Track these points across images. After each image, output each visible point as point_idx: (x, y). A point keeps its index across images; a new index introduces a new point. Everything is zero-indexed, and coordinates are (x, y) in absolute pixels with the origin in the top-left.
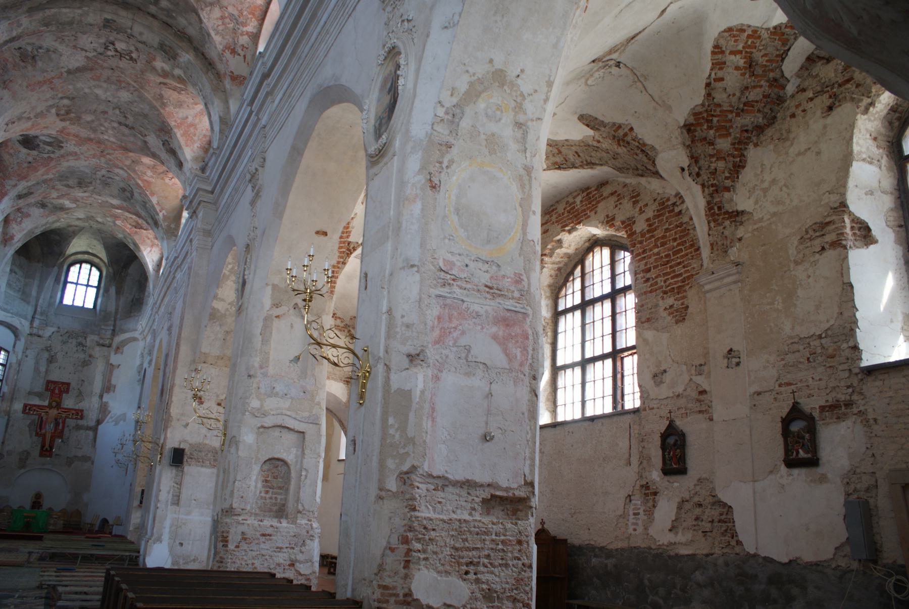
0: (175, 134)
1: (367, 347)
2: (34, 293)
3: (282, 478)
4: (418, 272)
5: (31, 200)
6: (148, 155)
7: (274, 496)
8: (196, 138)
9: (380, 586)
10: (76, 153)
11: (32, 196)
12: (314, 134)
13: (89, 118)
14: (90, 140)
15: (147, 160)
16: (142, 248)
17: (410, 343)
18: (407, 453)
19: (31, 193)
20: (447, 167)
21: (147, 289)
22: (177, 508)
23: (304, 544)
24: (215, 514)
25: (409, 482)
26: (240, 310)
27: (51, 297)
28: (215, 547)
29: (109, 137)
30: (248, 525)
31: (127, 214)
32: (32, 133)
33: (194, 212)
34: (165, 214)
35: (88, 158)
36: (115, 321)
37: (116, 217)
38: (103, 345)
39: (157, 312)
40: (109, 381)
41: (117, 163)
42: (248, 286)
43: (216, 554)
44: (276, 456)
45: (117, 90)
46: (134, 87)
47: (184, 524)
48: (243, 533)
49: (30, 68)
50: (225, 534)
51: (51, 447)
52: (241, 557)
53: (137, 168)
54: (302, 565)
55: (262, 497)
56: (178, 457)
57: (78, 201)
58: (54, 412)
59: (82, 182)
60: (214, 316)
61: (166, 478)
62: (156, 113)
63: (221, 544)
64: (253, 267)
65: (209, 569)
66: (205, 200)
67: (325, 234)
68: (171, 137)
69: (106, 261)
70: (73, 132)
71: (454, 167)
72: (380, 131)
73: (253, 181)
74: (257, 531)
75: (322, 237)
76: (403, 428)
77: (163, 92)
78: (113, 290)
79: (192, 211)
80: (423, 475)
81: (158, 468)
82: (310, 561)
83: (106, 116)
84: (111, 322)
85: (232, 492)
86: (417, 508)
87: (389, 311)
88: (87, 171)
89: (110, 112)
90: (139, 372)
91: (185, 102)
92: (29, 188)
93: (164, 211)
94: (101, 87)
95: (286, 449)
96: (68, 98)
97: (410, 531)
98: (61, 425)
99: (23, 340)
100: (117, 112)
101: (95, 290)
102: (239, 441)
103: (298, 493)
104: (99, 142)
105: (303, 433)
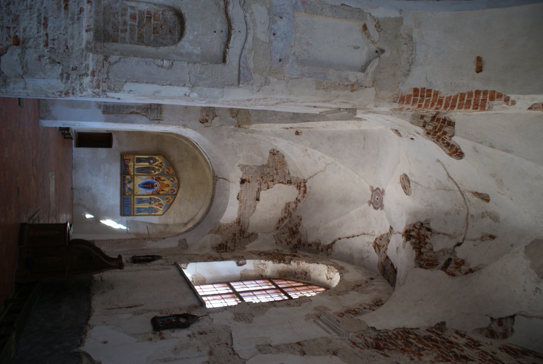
44: (187, 24)
55: (125, 9)
67: (479, 70)
105: (224, 61)
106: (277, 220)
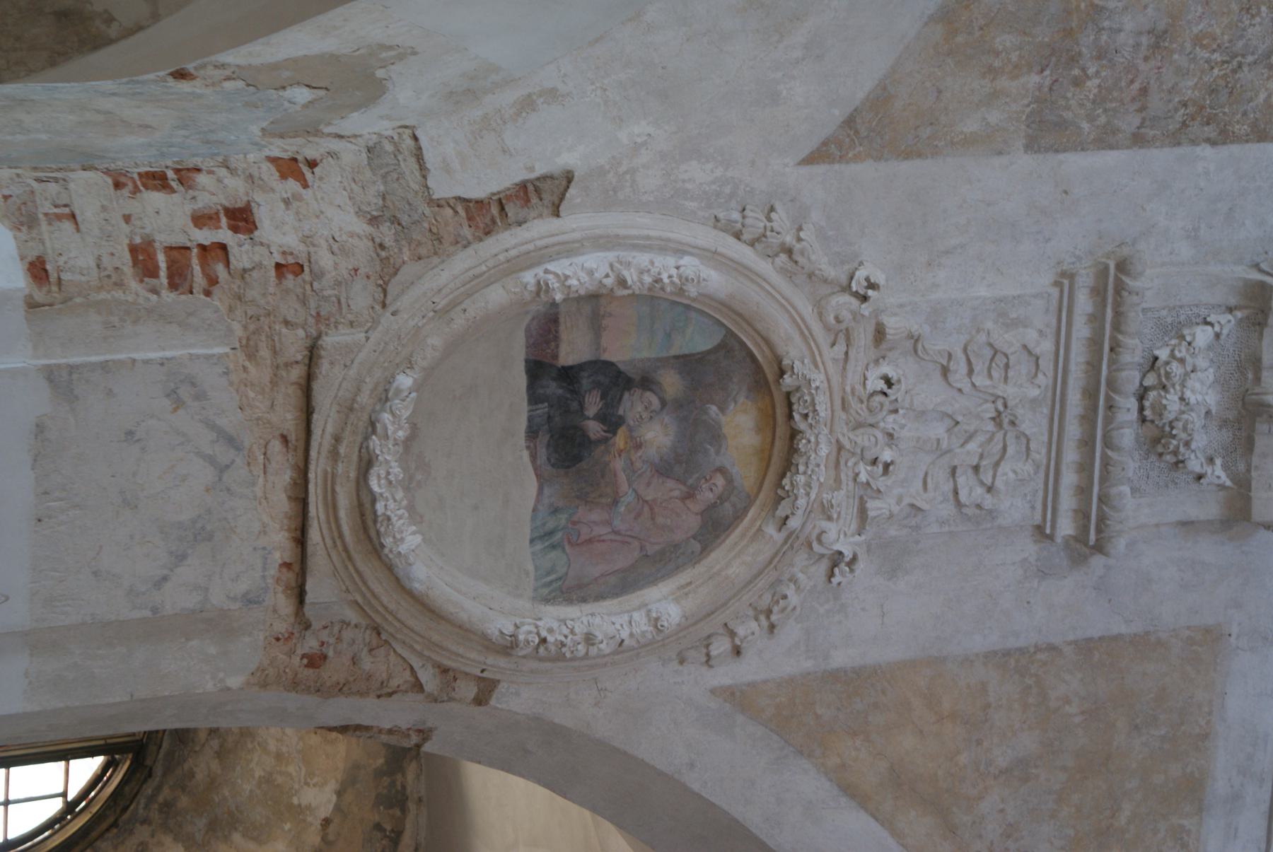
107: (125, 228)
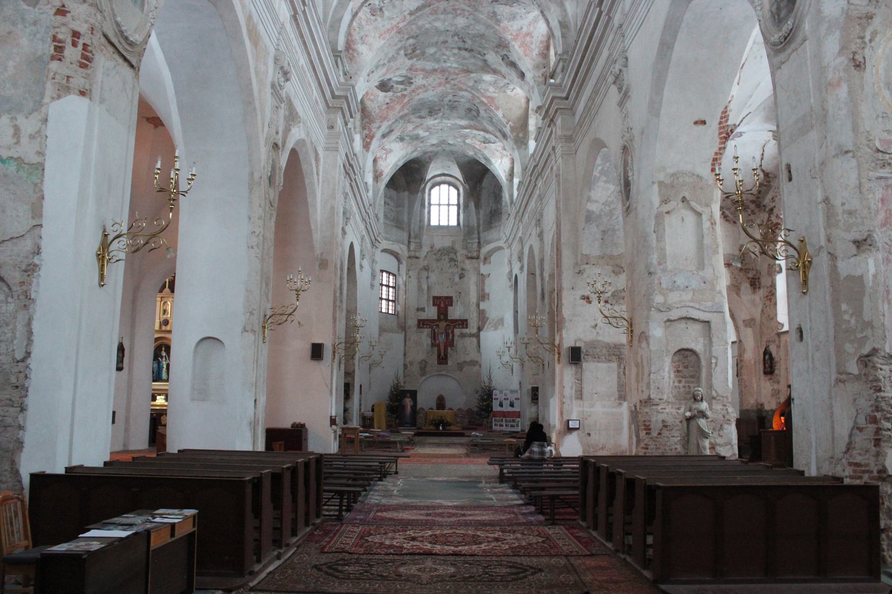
0: (513, 46)
1: (804, 237)
2: (406, 219)
3: (693, 367)
4: (853, 157)
5: (393, 136)
6: (488, 72)
7: (687, 385)
8: (533, 46)
9: (850, 464)
10: (424, 86)
11: (393, 133)
12: (683, 25)
13: (431, 50)
14: (435, 70)
15: (488, 78)
16: (493, 161)
17: (855, 229)
18: (865, 337)
19: (392, 131)
20: (871, 41)
21: (503, 199)
22: (581, 402)
23: (721, 428)
24: (632, 405)
25: (871, 364)
26: (628, 210)
27: (420, 221)
28: (638, 436)
29: (452, 64)
30: (667, 413)
31: (475, 132)
32: (387, 77)
33: (552, 120)
34: (512, 125)
35: (435, 87)
36: (479, 233)
37: (465, 137)
38: (472, 258)
39: (520, 220)
40: (483, 290)
41: (461, 86)
42: (634, 188)
43: (639, 441)
44: (685, 347)
45: (454, 18)
46: (468, 11)
47: (590, 416)
48: (663, 421)
49: (379, 19)
50: (647, 423)
51: (446, 356)
52: (664, 443)
53: (479, 87)
54: (721, 448)
55: (675, 387)
56: (575, 355)
57: (430, 128)
58: (443, 324)
59: (433, 111)
60: (589, 218)
61: (566, 375)
62: (492, 31)
63: (645, 432)
64: (635, 168)
65: (634, 454)
66: (562, 107)
68: (509, 51)
69: (461, 179)
70: (419, 67)
71: (877, 39)
72: (778, 16)
73: (618, 83)
74: (676, 418)
75: (701, 127)
76: (858, 312)
77: (496, 10)
78: (472, 205)
79: (549, 120)
80: (885, 357)
81: (558, 367)
82: (729, 443)
83: (446, 45)
84: (476, 236)
85: (648, 384)
86: (883, 389)
87: (826, 200)
88: (436, 100)
89: (450, 40)
90: (510, 279)
91: (517, 13)
92: (390, 126)
93: (510, 123)
94: (439, 19)
95: (693, 339)
96: (412, 37)
97: (878, 411)
98: (451, 335)
99: (404, 263)
100: (456, 38)
101: (456, 208)
102: (649, 336)
103: (711, 380)
104: (443, 71)
105: (708, 322)
106: (727, 223)
107: (74, 65)
